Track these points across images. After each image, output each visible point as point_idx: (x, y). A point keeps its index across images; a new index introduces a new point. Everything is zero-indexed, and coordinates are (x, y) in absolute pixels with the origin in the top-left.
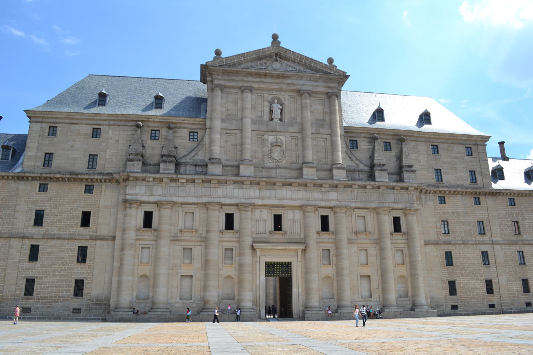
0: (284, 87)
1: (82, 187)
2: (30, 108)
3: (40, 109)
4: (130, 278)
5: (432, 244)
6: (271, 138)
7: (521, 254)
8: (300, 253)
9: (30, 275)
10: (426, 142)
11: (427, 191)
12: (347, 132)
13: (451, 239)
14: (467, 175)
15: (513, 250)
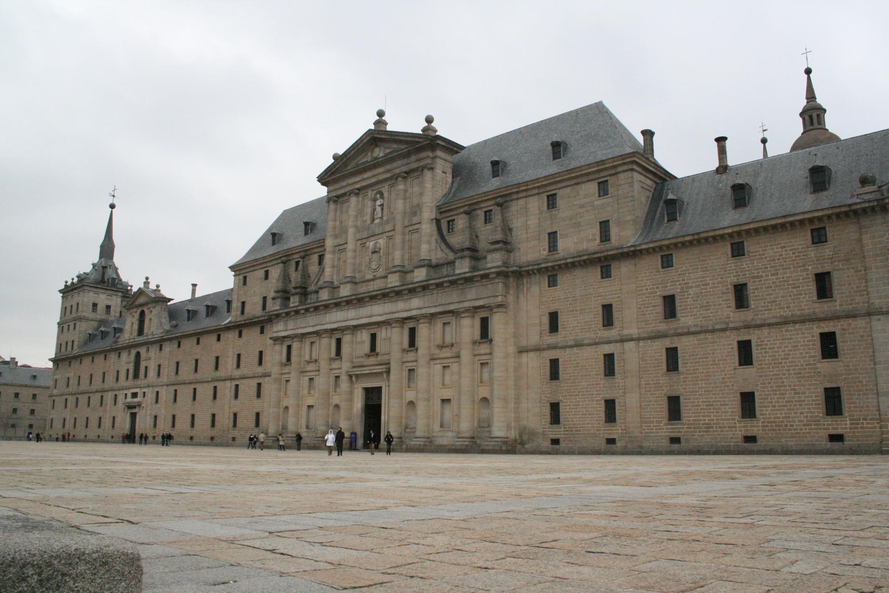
0: (381, 177)
1: (258, 330)
2: (231, 264)
3: (252, 257)
4: (276, 410)
5: (531, 350)
6: (371, 244)
7: (672, 355)
8: (385, 376)
9: (235, 410)
10: (538, 194)
11: (528, 272)
12: (445, 212)
13: (559, 340)
14: (595, 231)
15: (658, 349)
